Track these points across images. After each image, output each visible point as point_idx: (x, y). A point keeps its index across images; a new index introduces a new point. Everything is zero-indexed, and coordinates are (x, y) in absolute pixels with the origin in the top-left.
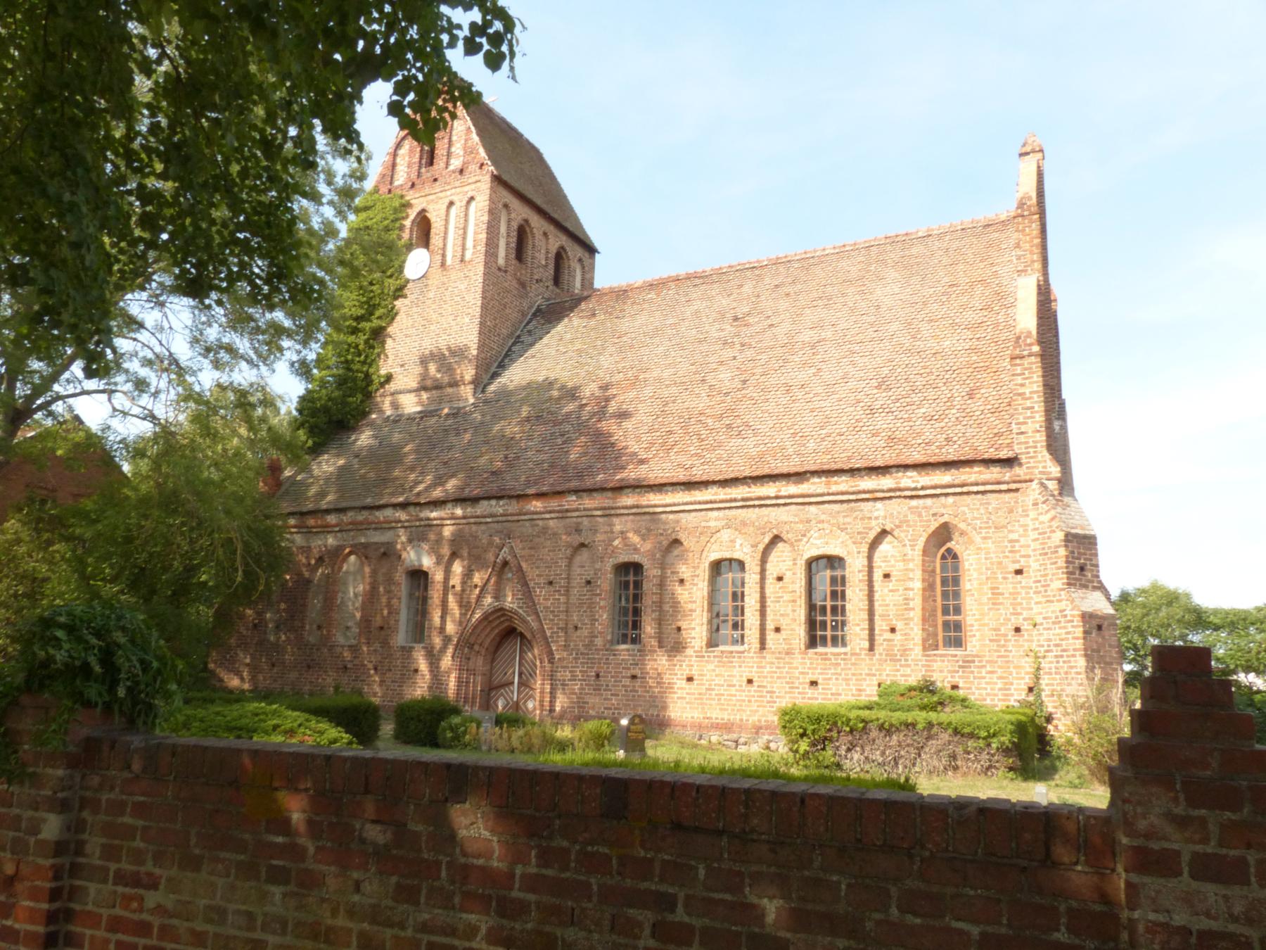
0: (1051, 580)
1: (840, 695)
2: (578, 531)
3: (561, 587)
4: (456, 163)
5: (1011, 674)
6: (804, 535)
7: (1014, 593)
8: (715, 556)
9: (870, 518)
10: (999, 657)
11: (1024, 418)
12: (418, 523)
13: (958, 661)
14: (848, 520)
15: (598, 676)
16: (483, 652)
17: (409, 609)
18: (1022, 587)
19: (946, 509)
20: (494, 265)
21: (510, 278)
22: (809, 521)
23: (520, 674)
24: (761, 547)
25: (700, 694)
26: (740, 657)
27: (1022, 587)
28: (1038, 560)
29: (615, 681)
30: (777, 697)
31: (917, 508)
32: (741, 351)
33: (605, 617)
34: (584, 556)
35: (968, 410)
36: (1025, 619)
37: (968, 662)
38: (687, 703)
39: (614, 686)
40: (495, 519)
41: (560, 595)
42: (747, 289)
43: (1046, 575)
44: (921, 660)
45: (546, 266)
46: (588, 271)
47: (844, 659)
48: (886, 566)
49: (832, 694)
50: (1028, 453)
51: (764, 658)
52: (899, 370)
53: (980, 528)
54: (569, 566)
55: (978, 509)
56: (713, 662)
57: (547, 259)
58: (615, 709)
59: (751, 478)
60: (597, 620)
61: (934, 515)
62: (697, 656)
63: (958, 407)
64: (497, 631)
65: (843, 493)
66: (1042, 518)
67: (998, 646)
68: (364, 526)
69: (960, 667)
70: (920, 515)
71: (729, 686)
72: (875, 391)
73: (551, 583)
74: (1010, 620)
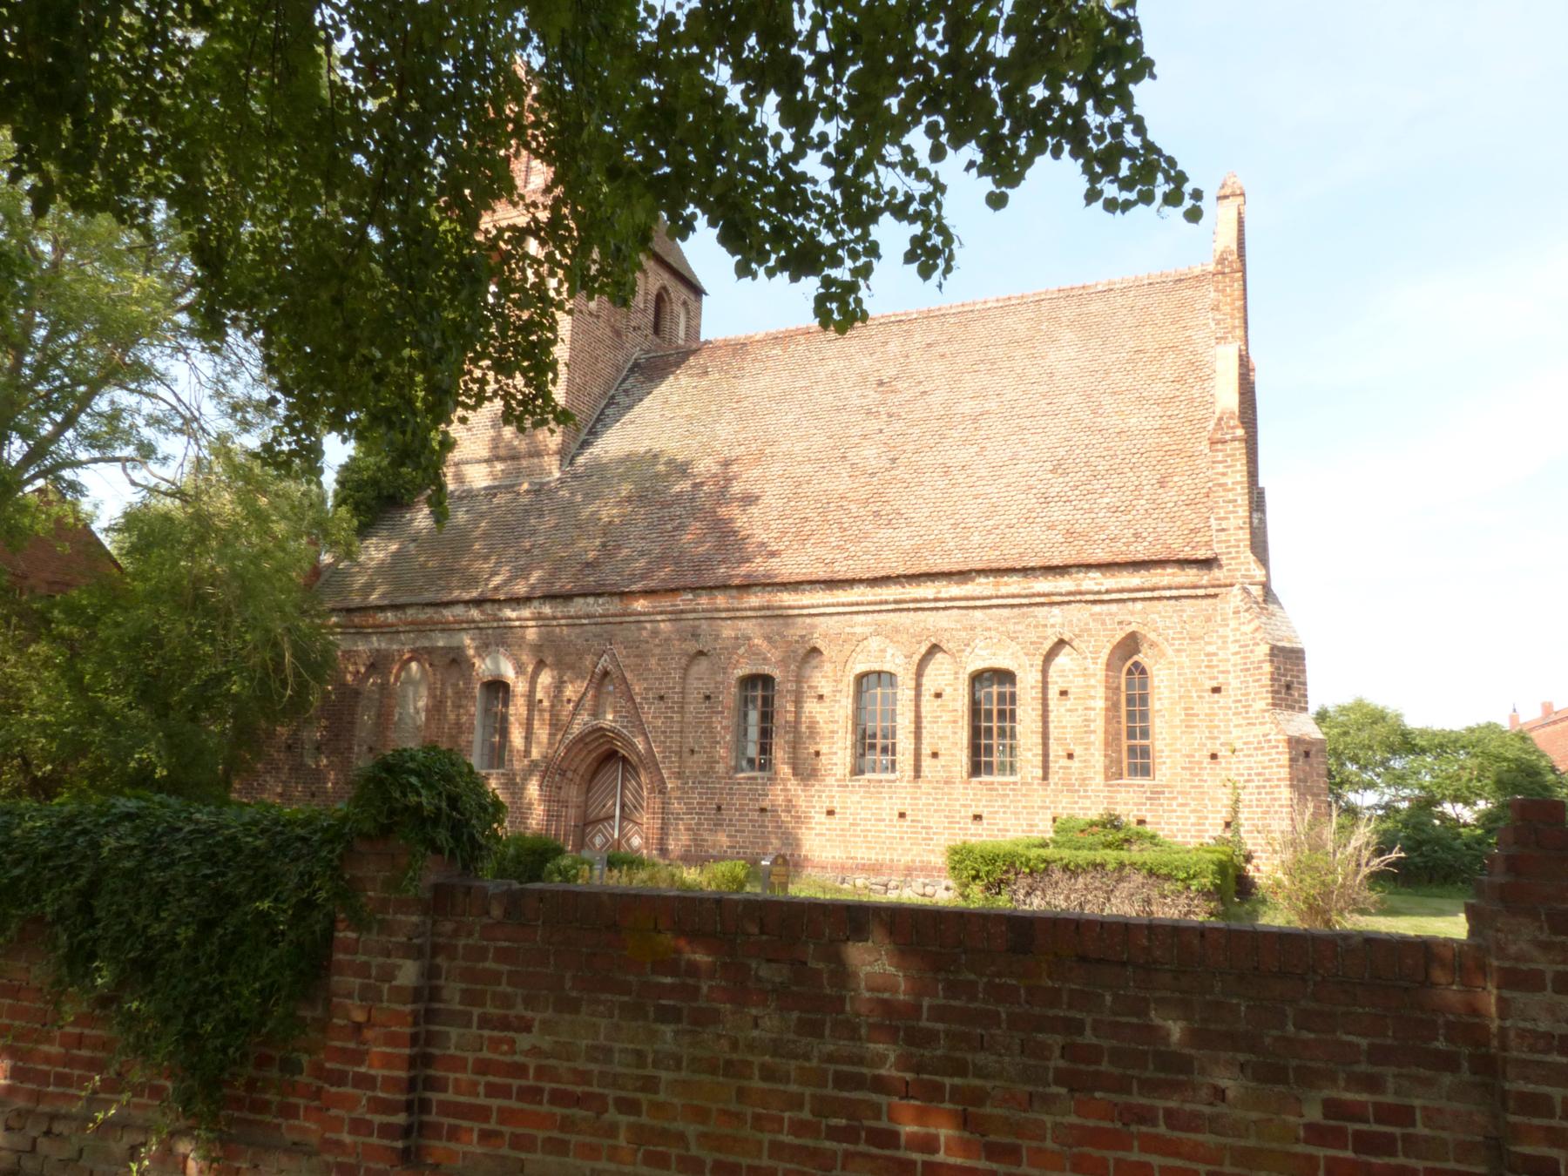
0: (1254, 700)
1: (1008, 831)
2: (695, 636)
3: (673, 703)
5: (1205, 806)
6: (967, 645)
8: (861, 668)
9: (1045, 626)
10: (1192, 787)
11: (1226, 513)
12: (495, 624)
13: (1145, 792)
14: (1020, 627)
15: (719, 808)
16: (578, 779)
17: (484, 727)
18: (1220, 708)
19: (1134, 617)
21: (602, 325)
22: (973, 628)
23: (623, 806)
24: (917, 658)
25: (842, 830)
27: (1220, 708)
28: (1239, 677)
30: (935, 833)
31: (1100, 614)
32: (888, 423)
33: (728, 738)
34: (703, 665)
36: (1222, 745)
37: (1157, 792)
38: (828, 840)
39: (739, 820)
40: (592, 621)
41: (673, 712)
42: (894, 347)
43: (1248, 694)
45: (645, 310)
46: (694, 316)
47: (1014, 790)
50: (1230, 553)
51: (920, 787)
52: (1078, 451)
54: (684, 678)
56: (858, 793)
57: (646, 301)
58: (741, 847)
59: (905, 576)
60: (719, 743)
61: (1120, 623)
64: (594, 755)
65: (1014, 596)
66: (1244, 628)
68: (428, 627)
69: (1148, 798)
70: (1104, 623)
71: (877, 820)
72: (1050, 476)
73: (661, 698)
74: (1205, 745)
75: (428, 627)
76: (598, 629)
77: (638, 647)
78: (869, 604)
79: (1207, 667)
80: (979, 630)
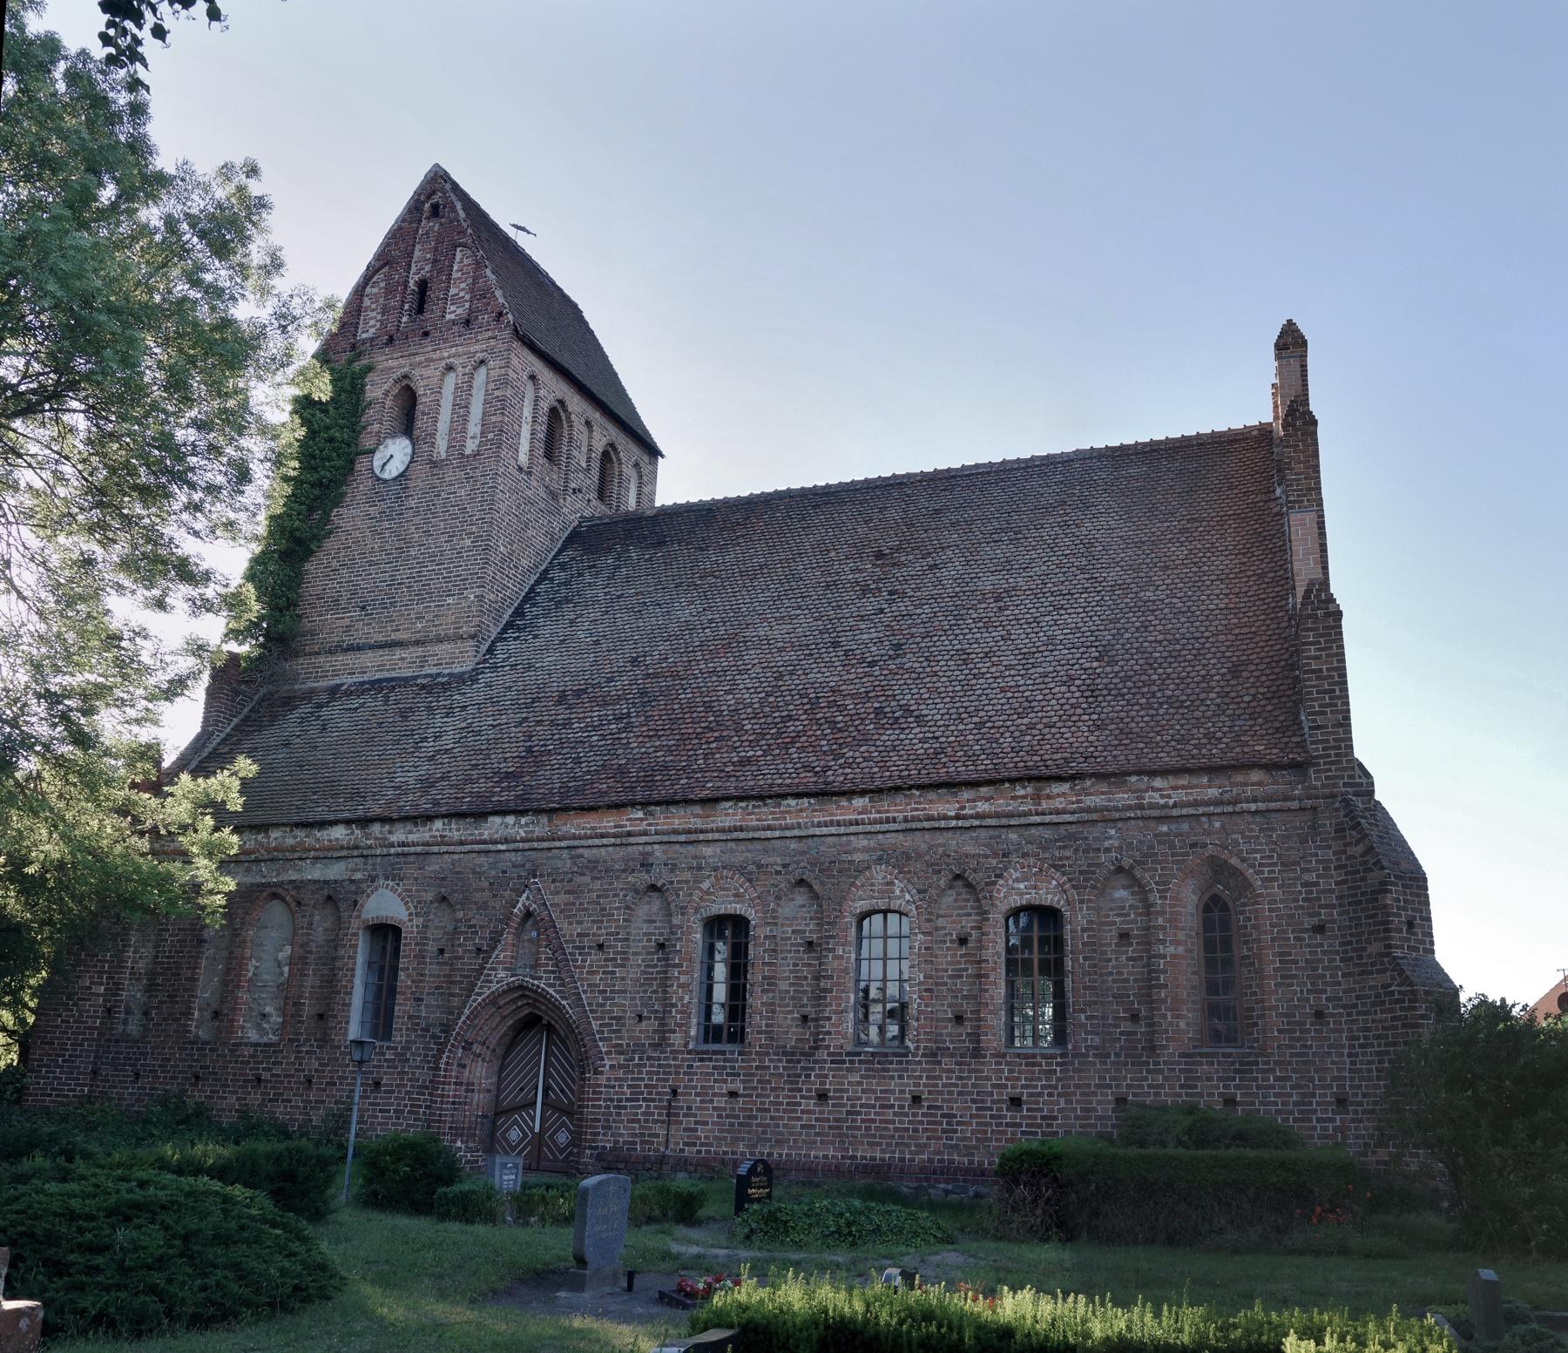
0: (1368, 941)
1: (1055, 1118)
2: (646, 866)
4: (454, 312)
5: (1312, 1080)
6: (1000, 876)
7: (1313, 961)
9: (1099, 850)
10: (1292, 1055)
11: (1320, 706)
12: (385, 851)
13: (1233, 1063)
14: (1068, 853)
15: (674, 1092)
17: (366, 985)
18: (1324, 952)
20: (512, 462)
21: (535, 483)
23: (546, 1089)
25: (836, 1120)
26: (900, 1062)
27: (1324, 952)
29: (702, 1102)
30: (959, 1123)
31: (1167, 834)
32: (891, 602)
34: (653, 906)
35: (1233, 694)
36: (1328, 999)
37: (1249, 1063)
38: (817, 1134)
39: (699, 1108)
40: (512, 846)
42: (893, 514)
43: (1361, 934)
44: (1179, 1063)
46: (647, 480)
48: (1123, 922)
49: (1043, 1118)
50: (1329, 756)
51: (939, 1063)
52: (1127, 635)
53: (1261, 865)
55: (1258, 837)
57: (589, 460)
58: (702, 1144)
60: (674, 1005)
61: (1194, 845)
62: (832, 1062)
63: (1218, 689)
65: (1058, 812)
66: (1351, 851)
67: (1291, 1039)
69: (1236, 1071)
71: (882, 1106)
72: (1095, 664)
73: (601, 947)
75: (297, 855)
76: (518, 858)
77: (571, 881)
78: (875, 822)
79: (1304, 900)
80: (1014, 858)
